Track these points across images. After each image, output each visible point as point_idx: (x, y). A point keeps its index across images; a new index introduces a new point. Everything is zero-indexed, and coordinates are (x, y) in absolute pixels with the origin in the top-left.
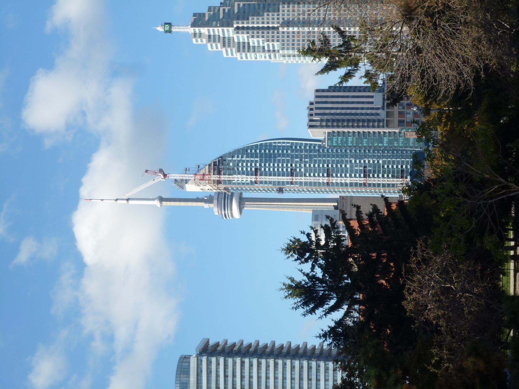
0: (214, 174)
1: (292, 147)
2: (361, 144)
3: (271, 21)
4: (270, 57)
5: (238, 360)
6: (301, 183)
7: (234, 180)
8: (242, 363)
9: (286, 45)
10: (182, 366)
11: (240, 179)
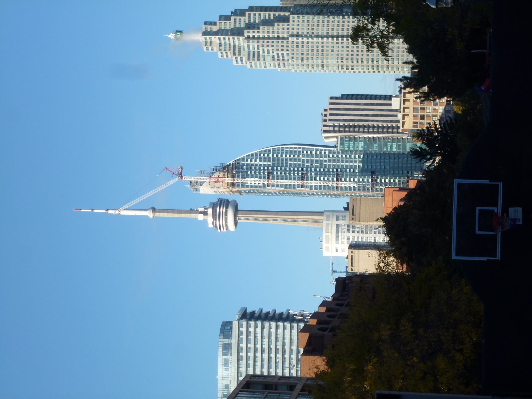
0: (228, 177)
1: (303, 152)
2: (372, 148)
3: (280, 31)
4: (279, 65)
5: (273, 324)
6: (311, 187)
7: (247, 183)
8: (277, 327)
9: (295, 54)
10: (224, 329)
11: (253, 182)
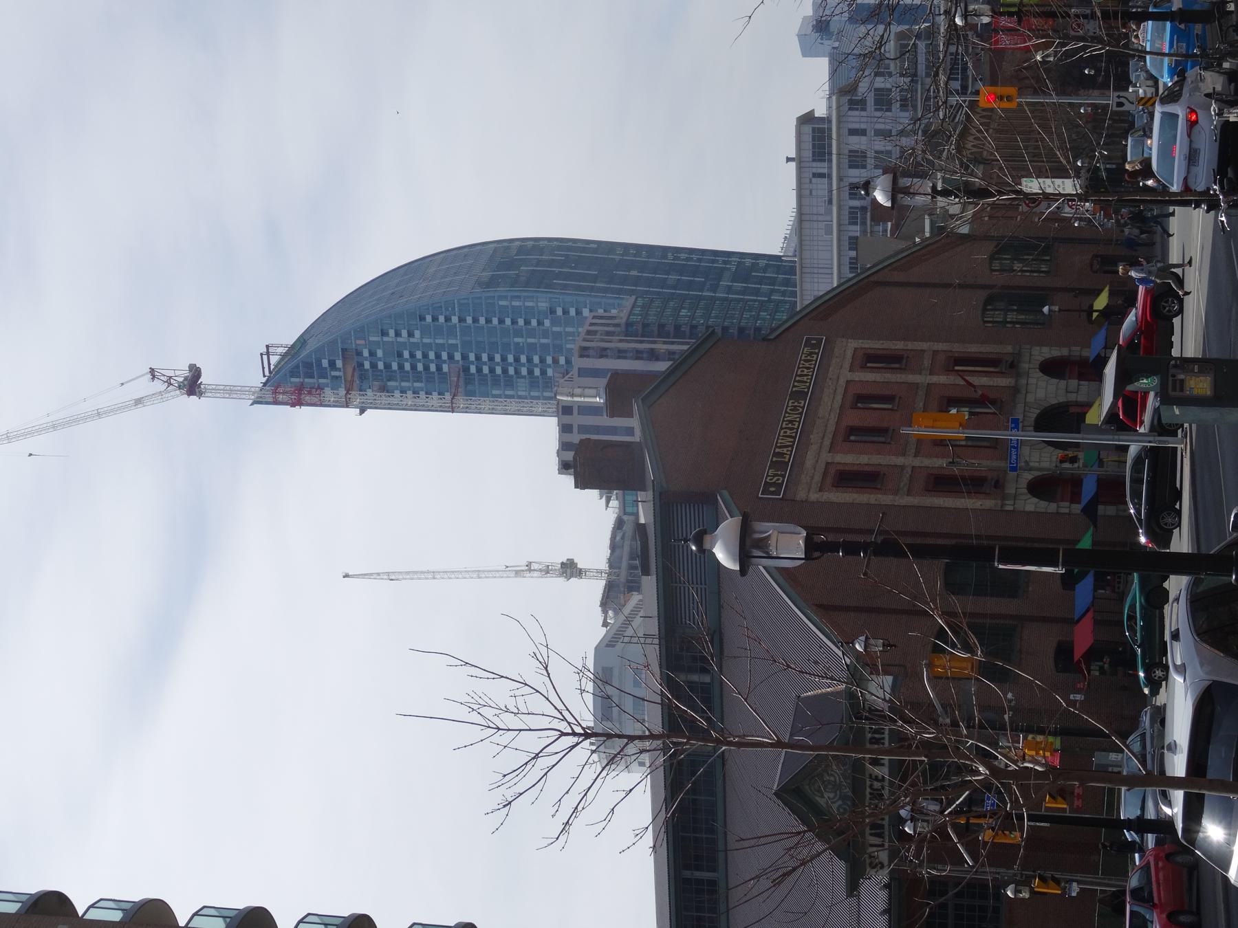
1: (553, 312)
